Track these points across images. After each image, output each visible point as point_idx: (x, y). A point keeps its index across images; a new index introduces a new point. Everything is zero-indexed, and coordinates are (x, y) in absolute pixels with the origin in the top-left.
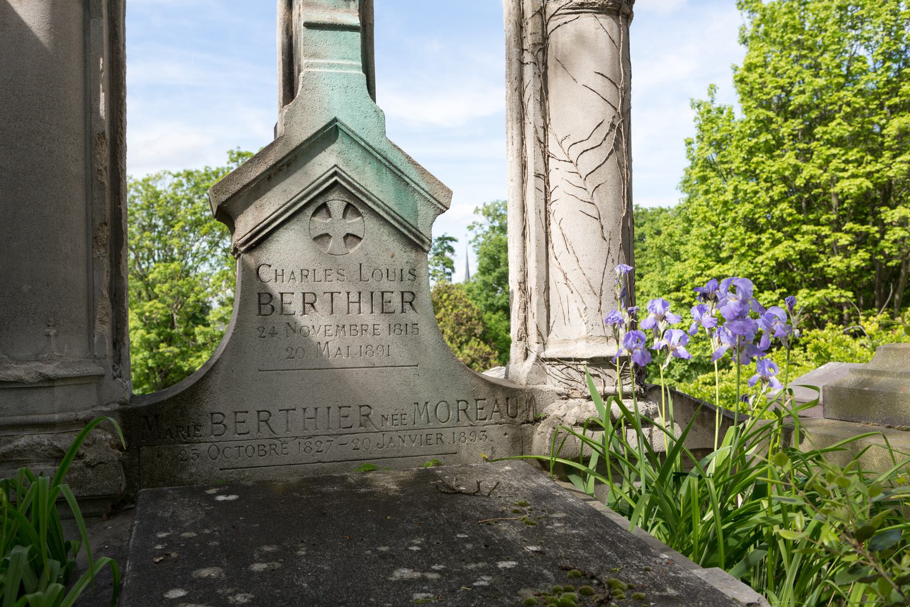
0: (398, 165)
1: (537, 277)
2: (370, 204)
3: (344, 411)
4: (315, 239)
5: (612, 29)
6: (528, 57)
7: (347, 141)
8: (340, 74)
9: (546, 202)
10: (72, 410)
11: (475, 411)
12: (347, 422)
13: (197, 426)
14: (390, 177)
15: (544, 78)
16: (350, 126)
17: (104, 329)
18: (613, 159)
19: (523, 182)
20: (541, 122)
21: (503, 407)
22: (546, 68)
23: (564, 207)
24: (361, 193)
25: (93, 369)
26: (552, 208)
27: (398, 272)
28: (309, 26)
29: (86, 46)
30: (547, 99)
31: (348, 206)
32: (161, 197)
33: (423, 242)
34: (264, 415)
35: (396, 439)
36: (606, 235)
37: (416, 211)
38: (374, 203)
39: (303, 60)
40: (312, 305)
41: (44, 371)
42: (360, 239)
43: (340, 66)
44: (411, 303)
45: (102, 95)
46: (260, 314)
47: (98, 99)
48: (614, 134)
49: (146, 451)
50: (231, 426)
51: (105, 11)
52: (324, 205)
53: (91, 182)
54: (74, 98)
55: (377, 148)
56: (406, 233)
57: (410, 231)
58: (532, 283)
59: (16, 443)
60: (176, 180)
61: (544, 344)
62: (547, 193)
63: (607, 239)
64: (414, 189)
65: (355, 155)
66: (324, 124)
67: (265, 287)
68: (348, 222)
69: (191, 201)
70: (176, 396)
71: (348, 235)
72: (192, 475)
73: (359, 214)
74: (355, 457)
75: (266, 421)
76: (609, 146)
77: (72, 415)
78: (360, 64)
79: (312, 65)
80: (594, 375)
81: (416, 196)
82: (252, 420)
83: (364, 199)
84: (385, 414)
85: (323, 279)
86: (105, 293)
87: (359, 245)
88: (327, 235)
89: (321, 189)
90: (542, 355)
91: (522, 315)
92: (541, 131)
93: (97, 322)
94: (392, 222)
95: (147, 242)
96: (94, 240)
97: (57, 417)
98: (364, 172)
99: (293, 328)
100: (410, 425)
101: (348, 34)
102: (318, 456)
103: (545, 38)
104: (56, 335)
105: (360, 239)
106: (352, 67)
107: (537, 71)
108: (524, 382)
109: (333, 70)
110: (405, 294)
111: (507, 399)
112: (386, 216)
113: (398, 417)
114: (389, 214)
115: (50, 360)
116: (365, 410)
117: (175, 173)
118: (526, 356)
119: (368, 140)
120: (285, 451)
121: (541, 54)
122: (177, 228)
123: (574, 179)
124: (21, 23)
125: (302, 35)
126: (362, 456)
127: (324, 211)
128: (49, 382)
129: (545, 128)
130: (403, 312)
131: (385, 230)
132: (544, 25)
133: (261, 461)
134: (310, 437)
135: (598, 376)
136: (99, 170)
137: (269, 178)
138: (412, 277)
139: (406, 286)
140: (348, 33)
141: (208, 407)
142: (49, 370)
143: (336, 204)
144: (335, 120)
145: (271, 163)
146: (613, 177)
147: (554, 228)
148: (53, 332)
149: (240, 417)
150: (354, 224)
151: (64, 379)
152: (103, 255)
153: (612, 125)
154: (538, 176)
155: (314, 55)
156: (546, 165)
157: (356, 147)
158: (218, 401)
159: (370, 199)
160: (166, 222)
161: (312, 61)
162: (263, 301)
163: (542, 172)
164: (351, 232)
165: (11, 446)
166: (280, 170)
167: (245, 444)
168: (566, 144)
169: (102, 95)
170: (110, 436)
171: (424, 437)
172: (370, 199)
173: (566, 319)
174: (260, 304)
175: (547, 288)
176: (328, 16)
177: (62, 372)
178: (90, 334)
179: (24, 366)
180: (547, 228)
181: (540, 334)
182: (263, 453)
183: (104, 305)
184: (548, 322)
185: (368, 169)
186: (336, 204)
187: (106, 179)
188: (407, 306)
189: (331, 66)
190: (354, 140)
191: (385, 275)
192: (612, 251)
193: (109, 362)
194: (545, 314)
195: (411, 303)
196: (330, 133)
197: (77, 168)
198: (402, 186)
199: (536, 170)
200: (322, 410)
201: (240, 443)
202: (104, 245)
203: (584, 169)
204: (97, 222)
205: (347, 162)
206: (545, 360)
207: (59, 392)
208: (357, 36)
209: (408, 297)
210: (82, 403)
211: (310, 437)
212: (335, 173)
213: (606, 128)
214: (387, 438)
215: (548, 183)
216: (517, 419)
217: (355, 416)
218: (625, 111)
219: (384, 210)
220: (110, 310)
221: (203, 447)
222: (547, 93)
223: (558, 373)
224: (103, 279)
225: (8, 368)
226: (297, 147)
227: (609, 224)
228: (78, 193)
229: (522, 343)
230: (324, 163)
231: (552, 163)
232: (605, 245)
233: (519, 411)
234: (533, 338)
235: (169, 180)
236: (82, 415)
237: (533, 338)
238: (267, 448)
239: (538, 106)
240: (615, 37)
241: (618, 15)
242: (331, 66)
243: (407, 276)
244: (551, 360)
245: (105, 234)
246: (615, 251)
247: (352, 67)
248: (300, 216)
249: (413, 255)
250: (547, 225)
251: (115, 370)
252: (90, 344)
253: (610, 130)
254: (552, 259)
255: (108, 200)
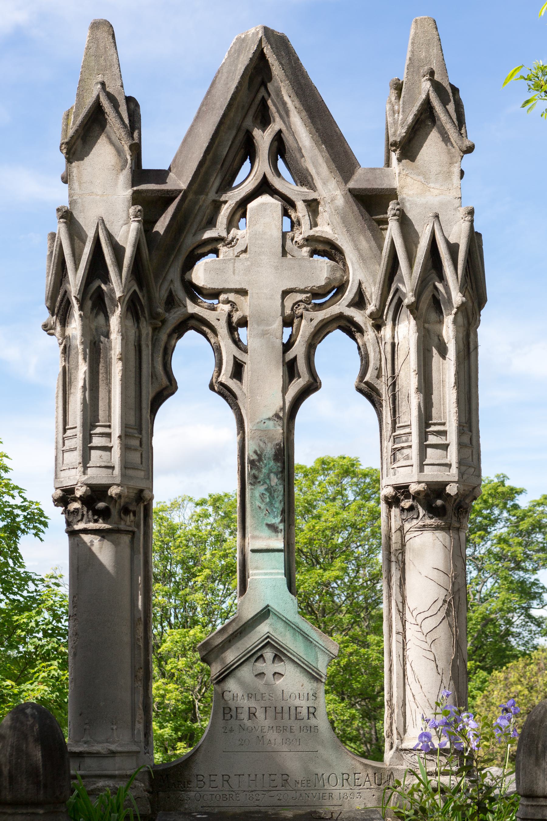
0: (306, 631)
1: (397, 698)
2: (289, 654)
3: (273, 777)
4: (256, 676)
5: (444, 539)
6: (393, 558)
7: (275, 618)
8: (271, 579)
9: (404, 649)
10: (124, 769)
11: (353, 780)
12: (274, 784)
13: (189, 782)
14: (301, 637)
15: (403, 571)
16: (276, 609)
17: (140, 726)
18: (445, 622)
19: (390, 637)
20: (400, 599)
21: (372, 779)
22: (404, 564)
23: (412, 653)
24: (283, 648)
25: (135, 748)
26: (408, 653)
27: (306, 695)
28: (253, 551)
29: (132, 570)
30: (405, 583)
31: (276, 656)
32: (179, 532)
33: (321, 676)
34: (226, 778)
35: (304, 795)
36: (440, 671)
37: (317, 658)
38: (291, 654)
39: (251, 571)
40: (254, 714)
41: (111, 748)
42: (283, 675)
43: (271, 574)
44: (313, 714)
45: (140, 597)
46: (224, 719)
47: (138, 600)
48: (446, 606)
49: (161, 794)
50: (207, 783)
51: (142, 550)
52: (262, 656)
53: (134, 645)
54: (126, 600)
55: (292, 621)
56: (311, 671)
57: (313, 670)
58: (395, 701)
59: (98, 785)
60: (199, 509)
61: (402, 740)
62: (404, 644)
63: (441, 674)
64: (316, 645)
65: (280, 626)
66: (261, 609)
67: (227, 704)
68: (276, 665)
69: (220, 539)
70: (178, 765)
71: (275, 673)
72: (186, 809)
73: (282, 661)
74: (279, 804)
75: (227, 781)
76: (442, 614)
77: (124, 772)
78: (283, 571)
79: (255, 574)
80: (430, 760)
81: (317, 649)
82: (219, 779)
83: (285, 652)
84: (297, 780)
85: (260, 699)
86: (141, 706)
87: (282, 679)
88: (263, 673)
89: (260, 646)
90: (400, 747)
91: (389, 721)
92: (400, 606)
93: (136, 722)
94: (302, 665)
95: (160, 598)
96: (135, 677)
97: (117, 772)
98: (285, 635)
99: (242, 728)
100: (313, 787)
101: (276, 554)
102: (257, 803)
103: (403, 545)
104: (116, 729)
105: (283, 675)
106: (278, 574)
107: (398, 567)
108: (388, 764)
109: (267, 577)
110: (310, 709)
111: (375, 774)
112: (298, 661)
113: (305, 782)
114: (300, 660)
115: (113, 743)
116: (285, 777)
117: (197, 499)
118: (391, 747)
119: (287, 617)
120: (238, 799)
121: (400, 555)
122: (199, 579)
123: (420, 635)
124: (101, 564)
125: (250, 556)
126: (283, 804)
127: (261, 659)
128: (113, 754)
129: (404, 603)
130: (308, 719)
131: (298, 670)
132: (403, 537)
133: (224, 804)
134: (252, 791)
135: (433, 760)
136: (138, 639)
137: (230, 641)
138: (314, 698)
139: (310, 703)
140: (276, 553)
141: (195, 771)
142: (113, 747)
143: (269, 654)
144: (268, 606)
145: (231, 632)
146: (445, 634)
147: (408, 666)
148: (115, 727)
149: (213, 778)
150: (279, 667)
151: (120, 752)
152: (140, 685)
153: (445, 601)
154: (398, 633)
155: (257, 568)
156: (404, 626)
157: (280, 621)
158: (201, 768)
159: (288, 652)
160: (187, 569)
161: (255, 572)
162: (226, 712)
163: (401, 630)
164: (277, 671)
165: (95, 786)
166: (236, 636)
167: (215, 793)
168: (415, 614)
169: (140, 597)
170: (143, 785)
171: (321, 795)
172: (288, 652)
173: (415, 725)
174: (224, 713)
175: (404, 704)
176: (265, 544)
177: (120, 749)
178: (133, 729)
179: (101, 745)
180: (404, 666)
181: (398, 733)
182: (225, 799)
183: (140, 713)
184: (405, 726)
185: (288, 633)
186: (269, 654)
187: (141, 644)
188: (311, 716)
189: (266, 574)
190: (279, 617)
191: (298, 697)
192: (444, 681)
193: (143, 744)
194: (402, 721)
195: (313, 714)
196: (265, 613)
197: (127, 639)
198: (308, 643)
199: (397, 629)
200: (259, 776)
201: (213, 793)
202: (140, 680)
203: (426, 630)
204: (137, 667)
205: (275, 630)
206: (402, 750)
207: (118, 759)
208: (281, 556)
209: (312, 710)
210: (128, 766)
211: (252, 791)
212: (268, 637)
213: (440, 603)
214: (298, 794)
215: (405, 638)
216: (381, 786)
217: (279, 780)
218: (456, 589)
219: (297, 658)
220: (143, 716)
221: (192, 794)
222: (404, 579)
223: (410, 758)
224: (140, 699)
225: (93, 746)
226: (246, 623)
227: (441, 664)
228: (127, 652)
229: (389, 739)
230: (264, 628)
231: (408, 625)
232: (439, 677)
233: (383, 782)
234: (395, 736)
235: (190, 510)
236: (129, 773)
237: (395, 736)
238: (228, 796)
239: (398, 589)
240: (447, 544)
241: (450, 529)
242: (266, 574)
243: (311, 697)
244: (405, 750)
245: (141, 674)
246: (446, 681)
247: (278, 574)
248: (247, 663)
249: (315, 684)
250: (404, 665)
251: (146, 749)
252: (133, 734)
253: (443, 604)
254: (407, 687)
255: (142, 655)
